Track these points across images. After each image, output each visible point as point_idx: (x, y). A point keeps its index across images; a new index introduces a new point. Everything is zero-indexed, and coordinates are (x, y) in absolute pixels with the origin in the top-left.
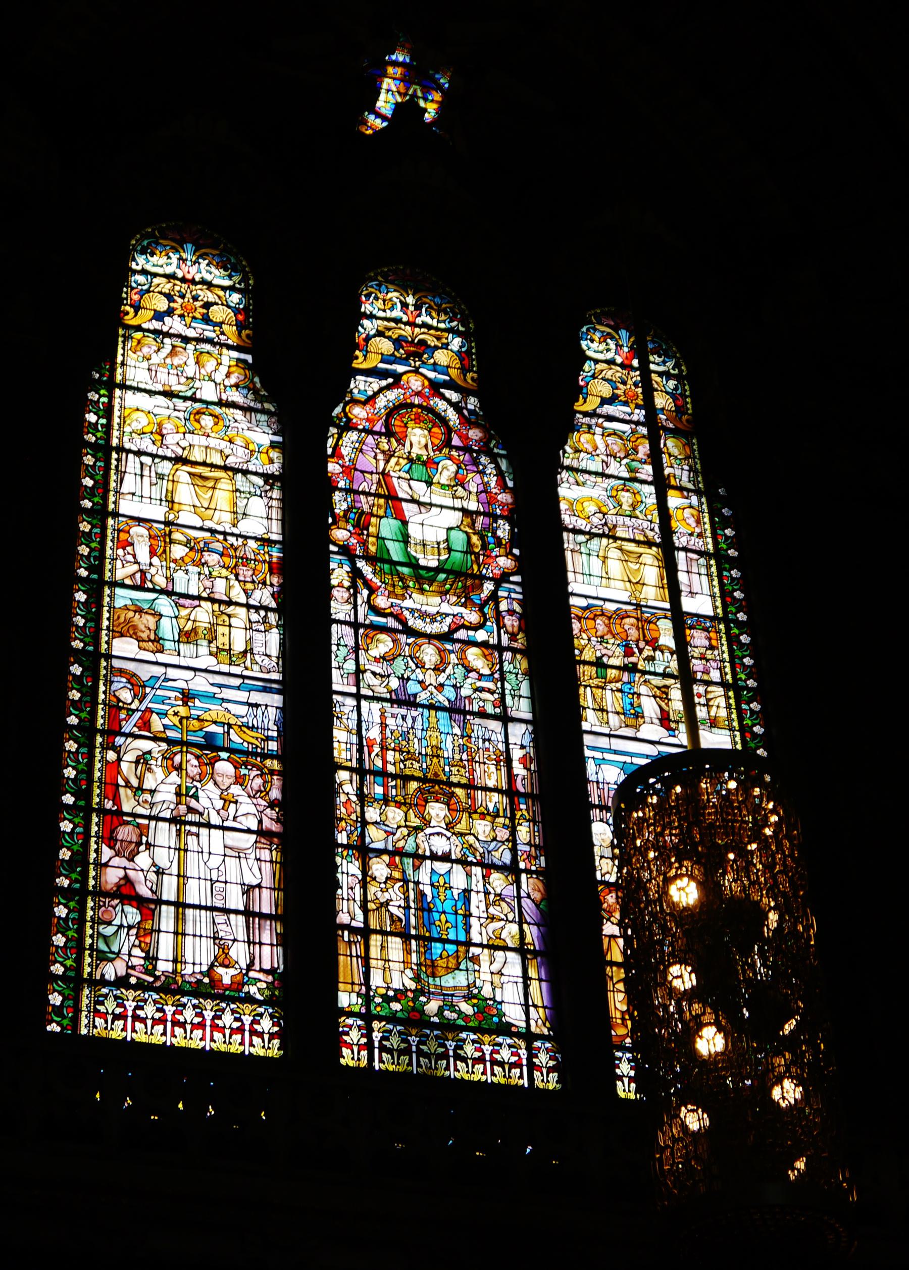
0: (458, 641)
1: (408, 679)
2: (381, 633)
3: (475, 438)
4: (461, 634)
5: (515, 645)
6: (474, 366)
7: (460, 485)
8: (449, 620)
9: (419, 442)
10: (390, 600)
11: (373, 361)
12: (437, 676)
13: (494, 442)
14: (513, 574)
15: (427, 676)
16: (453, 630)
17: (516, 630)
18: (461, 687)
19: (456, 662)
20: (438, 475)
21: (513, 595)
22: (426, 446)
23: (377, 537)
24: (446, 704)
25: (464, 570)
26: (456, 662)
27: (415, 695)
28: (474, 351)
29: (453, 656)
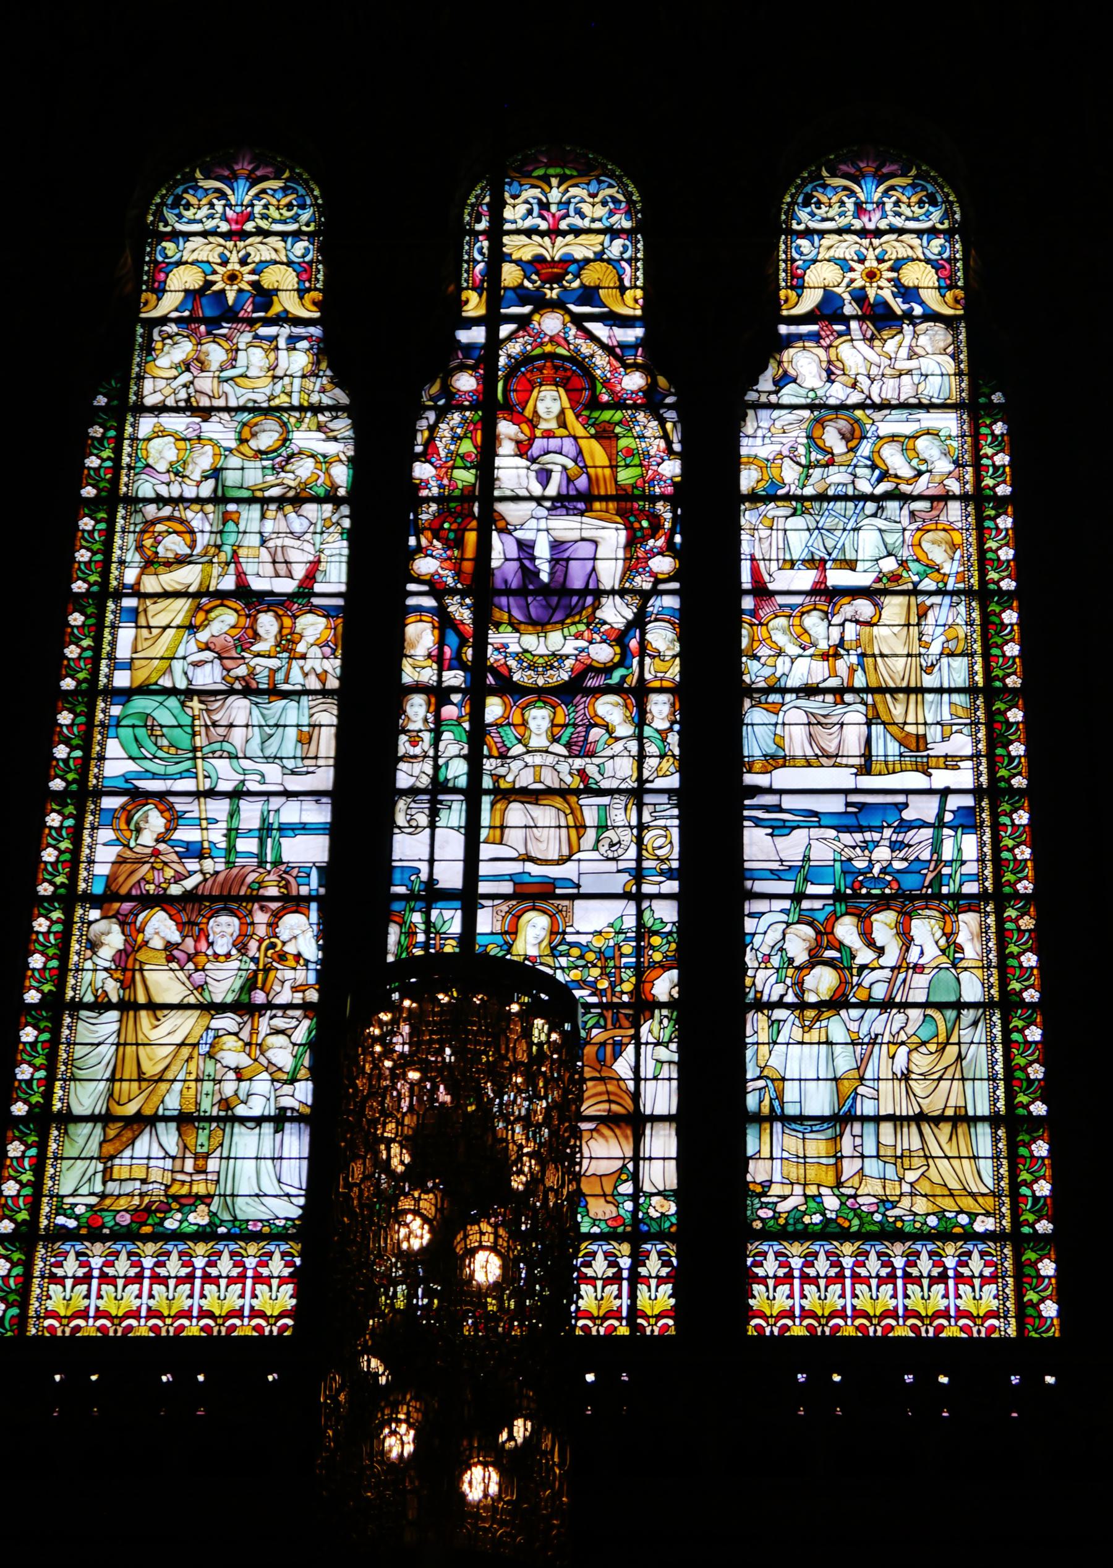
8: (569, 663)
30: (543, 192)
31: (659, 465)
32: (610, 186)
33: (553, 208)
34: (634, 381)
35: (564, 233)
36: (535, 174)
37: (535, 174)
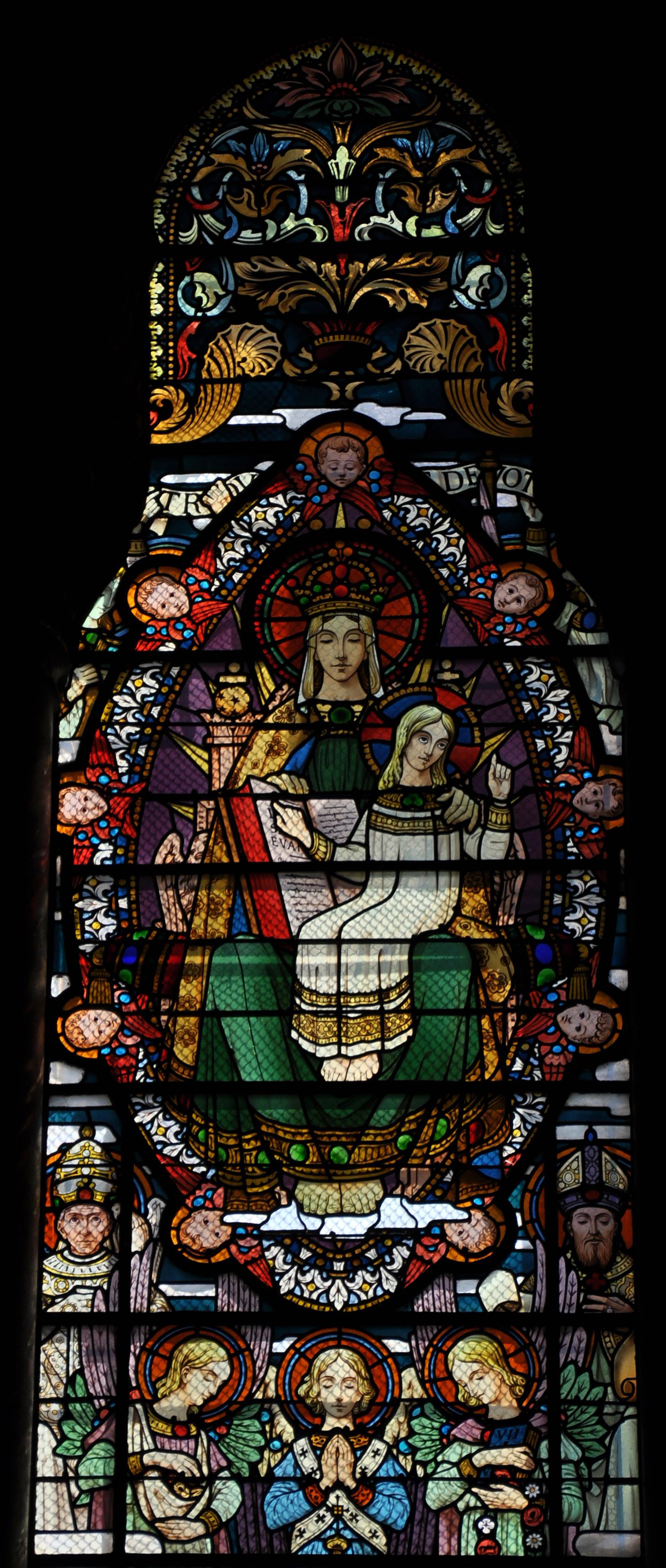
0: (429, 1318)
1: (271, 1478)
2: (197, 1337)
3: (514, 607)
5: (599, 1303)
6: (523, 353)
7: (460, 785)
9: (343, 659)
10: (229, 1219)
12: (358, 1452)
13: (570, 609)
14: (608, 1057)
15: (328, 1459)
17: (604, 1249)
18: (428, 1477)
19: (418, 1392)
20: (394, 761)
21: (603, 1132)
22: (363, 670)
23: (201, 1013)
24: (380, 1542)
25: (455, 1075)
26: (418, 1392)
27: (287, 1530)
29: (409, 1375)
30: (316, 155)
32: (460, 143)
33: (341, 194)
35: (363, 251)
36: (299, 114)
37: (299, 114)
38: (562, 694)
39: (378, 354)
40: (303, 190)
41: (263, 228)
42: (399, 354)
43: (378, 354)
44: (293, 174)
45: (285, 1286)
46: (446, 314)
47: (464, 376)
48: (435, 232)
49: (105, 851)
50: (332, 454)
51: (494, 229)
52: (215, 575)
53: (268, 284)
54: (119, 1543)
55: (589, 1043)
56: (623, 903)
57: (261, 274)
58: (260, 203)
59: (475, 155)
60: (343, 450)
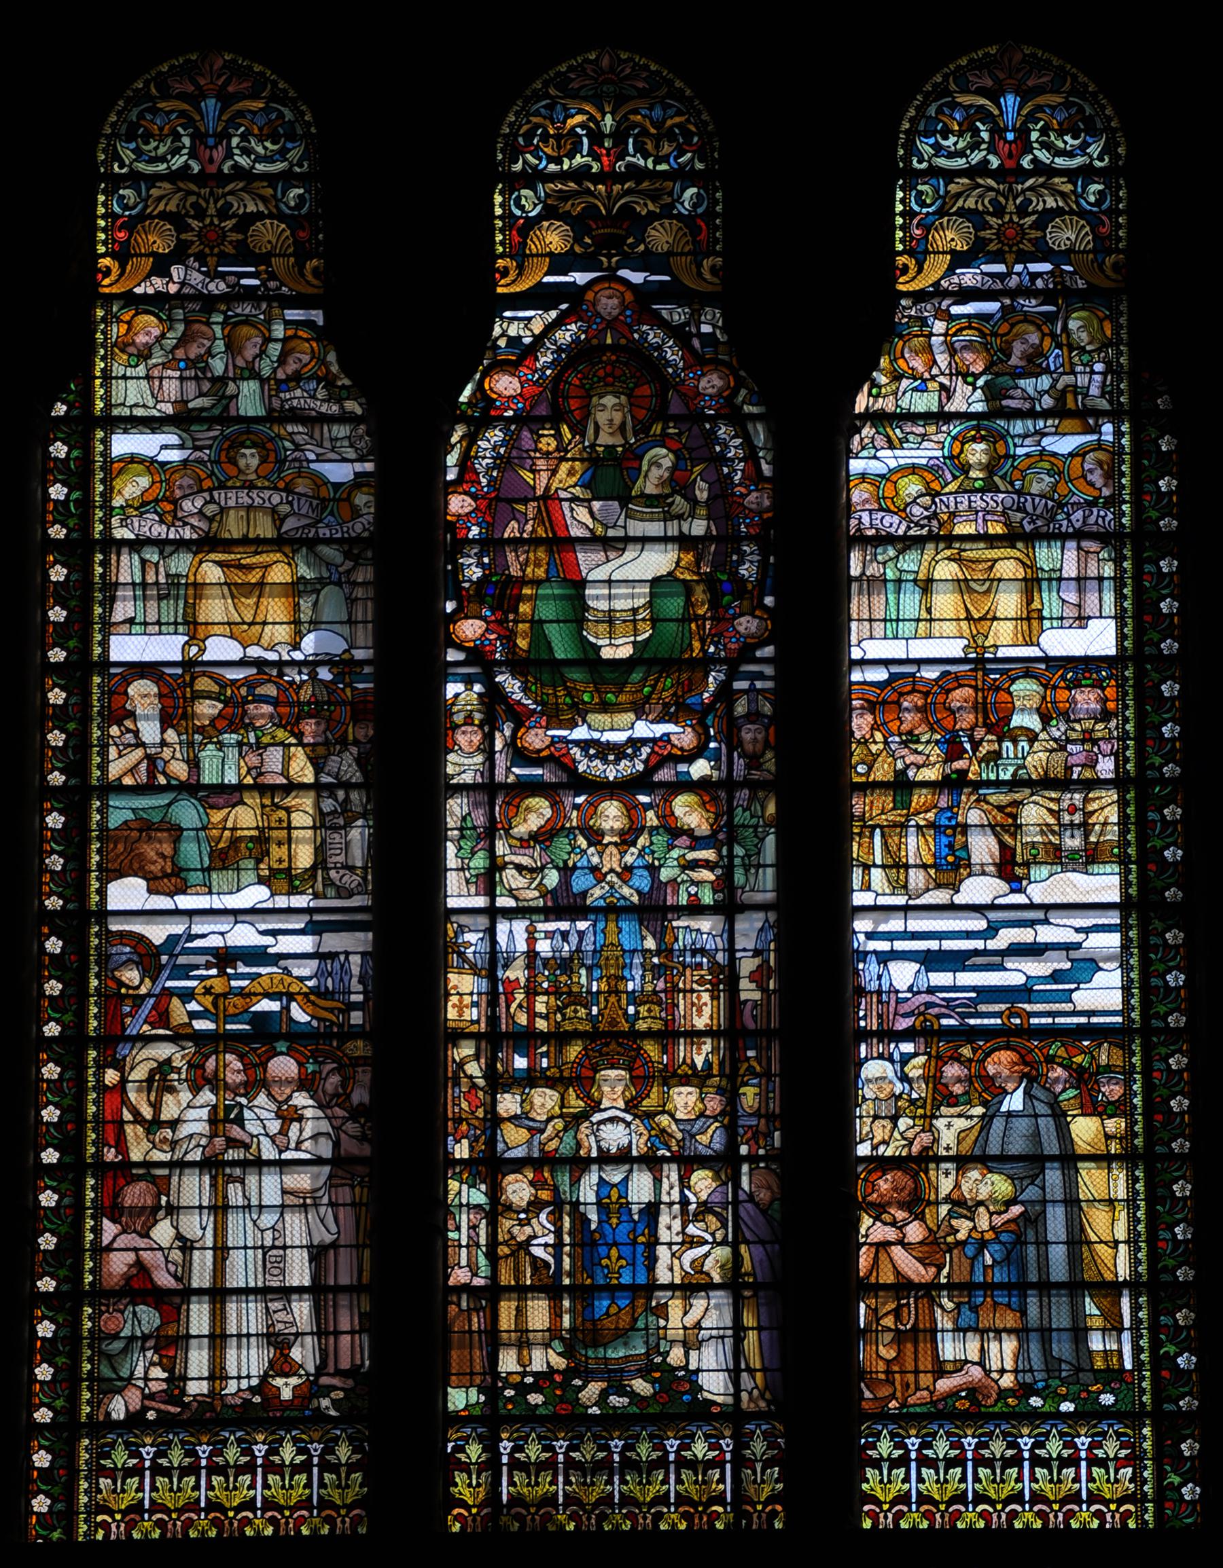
0: (661, 784)
1: (575, 867)
2: (533, 795)
3: (710, 391)
4: (664, 775)
5: (756, 775)
6: (716, 241)
7: (678, 493)
9: (611, 420)
10: (550, 733)
11: (539, 275)
12: (623, 854)
13: (743, 392)
14: (763, 644)
15: (606, 857)
16: (651, 769)
17: (759, 747)
18: (661, 866)
19: (656, 822)
20: (640, 481)
21: (759, 684)
22: (622, 428)
23: (532, 621)
24: (635, 899)
25: (676, 655)
26: (656, 822)
27: (584, 894)
28: (719, 208)
29: (650, 814)
31: (743, 496)
32: (679, 113)
34: (711, 383)
35: (621, 178)
36: (582, 93)
37: (582, 93)
38: (738, 441)
39: (630, 240)
40: (585, 140)
41: (561, 163)
42: (643, 241)
43: (630, 240)
44: (579, 130)
45: (581, 768)
46: (672, 217)
47: (682, 254)
48: (663, 167)
49: (475, 531)
50: (604, 300)
51: (699, 166)
52: (536, 371)
53: (564, 196)
54: (493, 901)
55: (752, 636)
56: (772, 559)
57: (561, 191)
58: (559, 147)
59: (688, 121)
60: (610, 297)
